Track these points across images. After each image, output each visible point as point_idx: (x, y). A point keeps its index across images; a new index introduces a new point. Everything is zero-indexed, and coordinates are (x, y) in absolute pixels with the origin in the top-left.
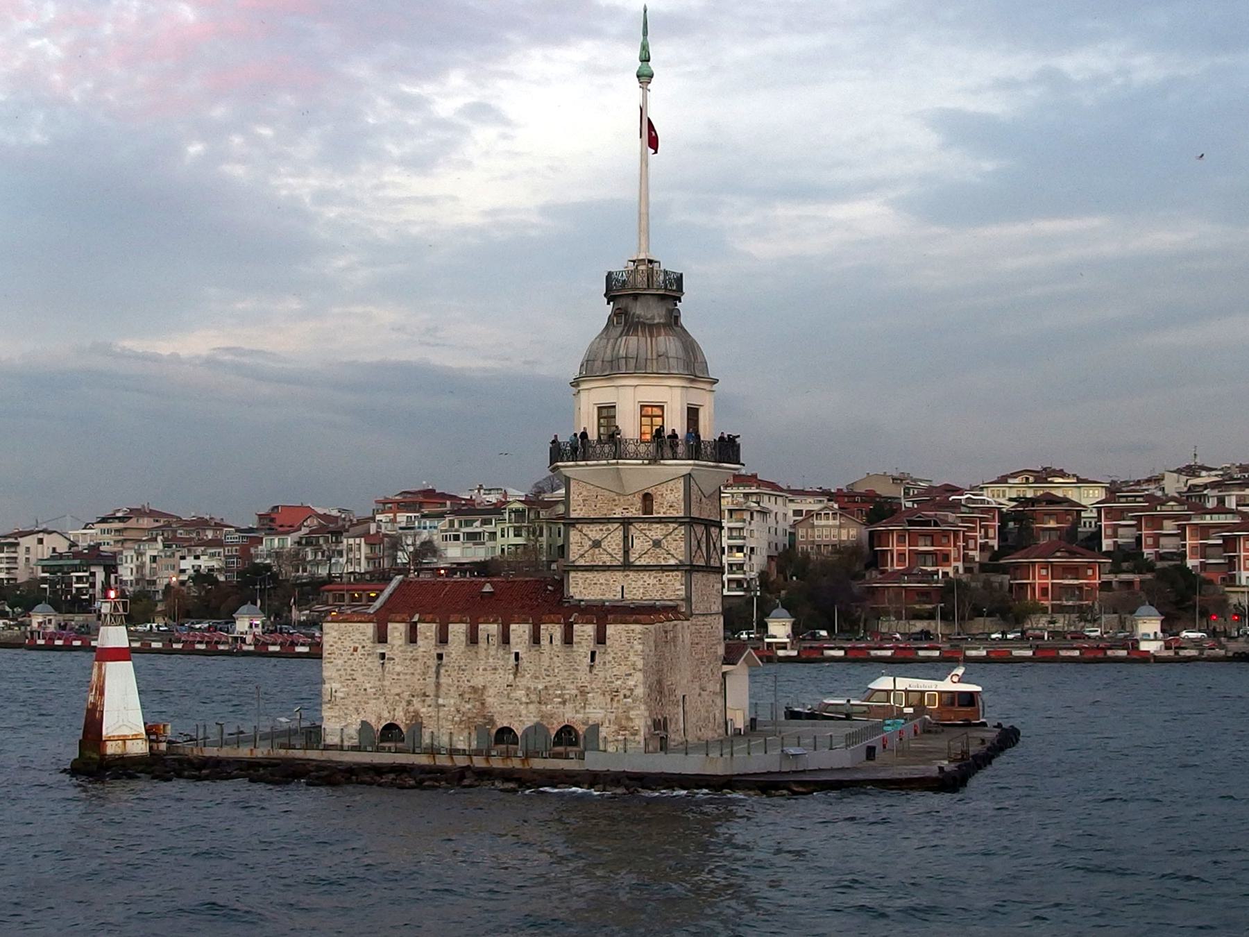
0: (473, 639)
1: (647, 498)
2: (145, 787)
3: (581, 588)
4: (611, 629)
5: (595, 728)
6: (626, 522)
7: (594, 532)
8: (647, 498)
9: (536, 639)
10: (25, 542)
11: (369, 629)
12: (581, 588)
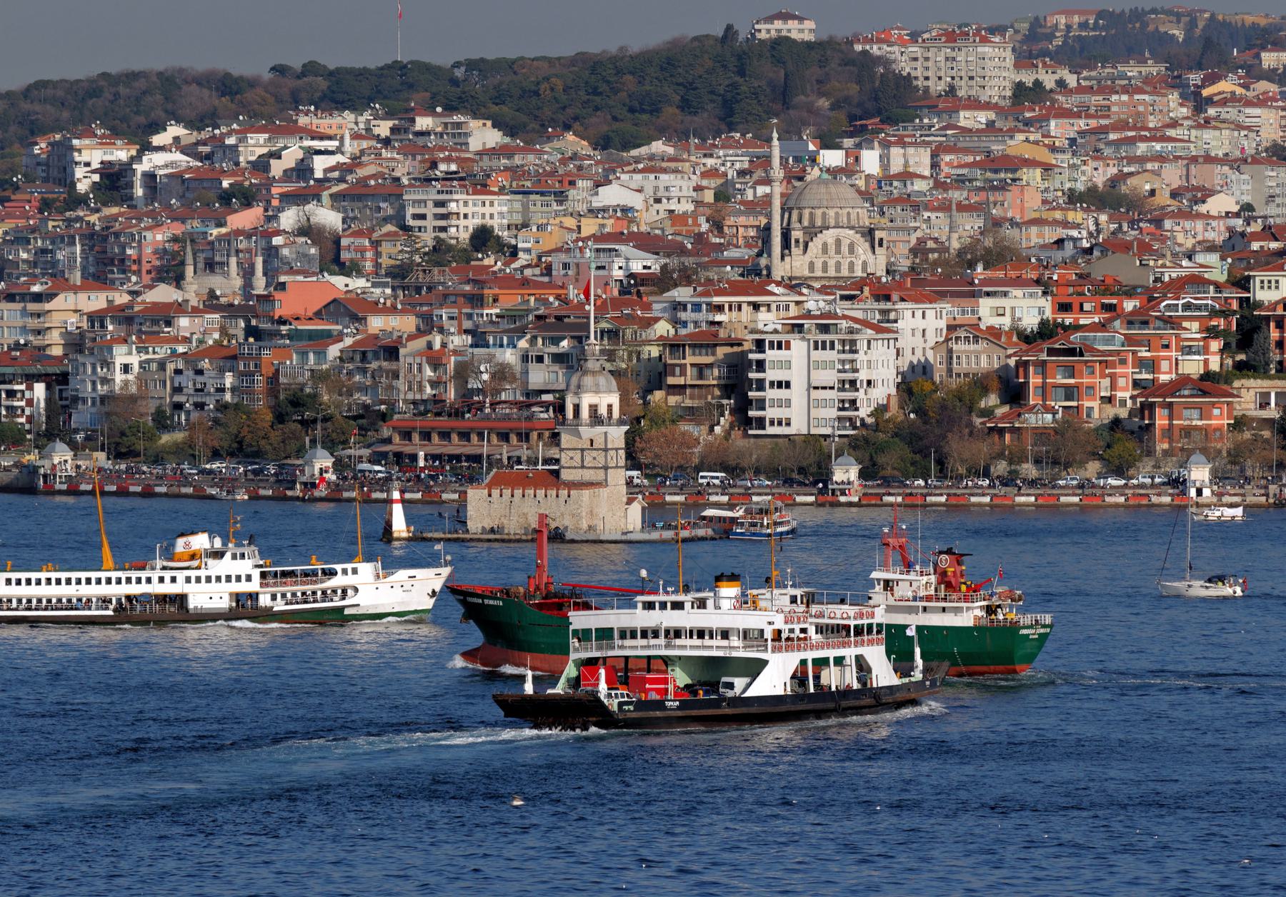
1: (592, 441)
6: (582, 450)
7: (571, 453)
8: (592, 441)
12: (566, 475)
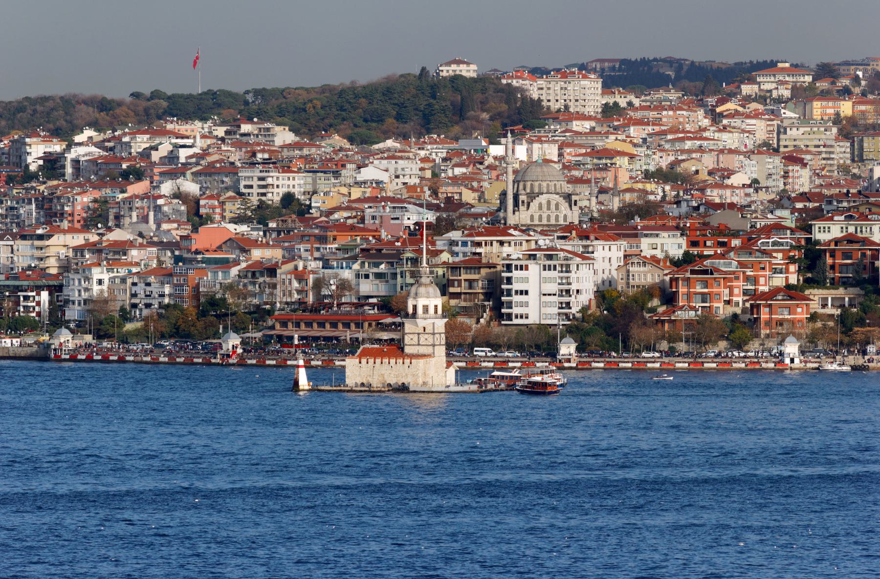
4: (413, 361)
6: (419, 334)
7: (411, 336)
11: (358, 360)
12: (407, 350)
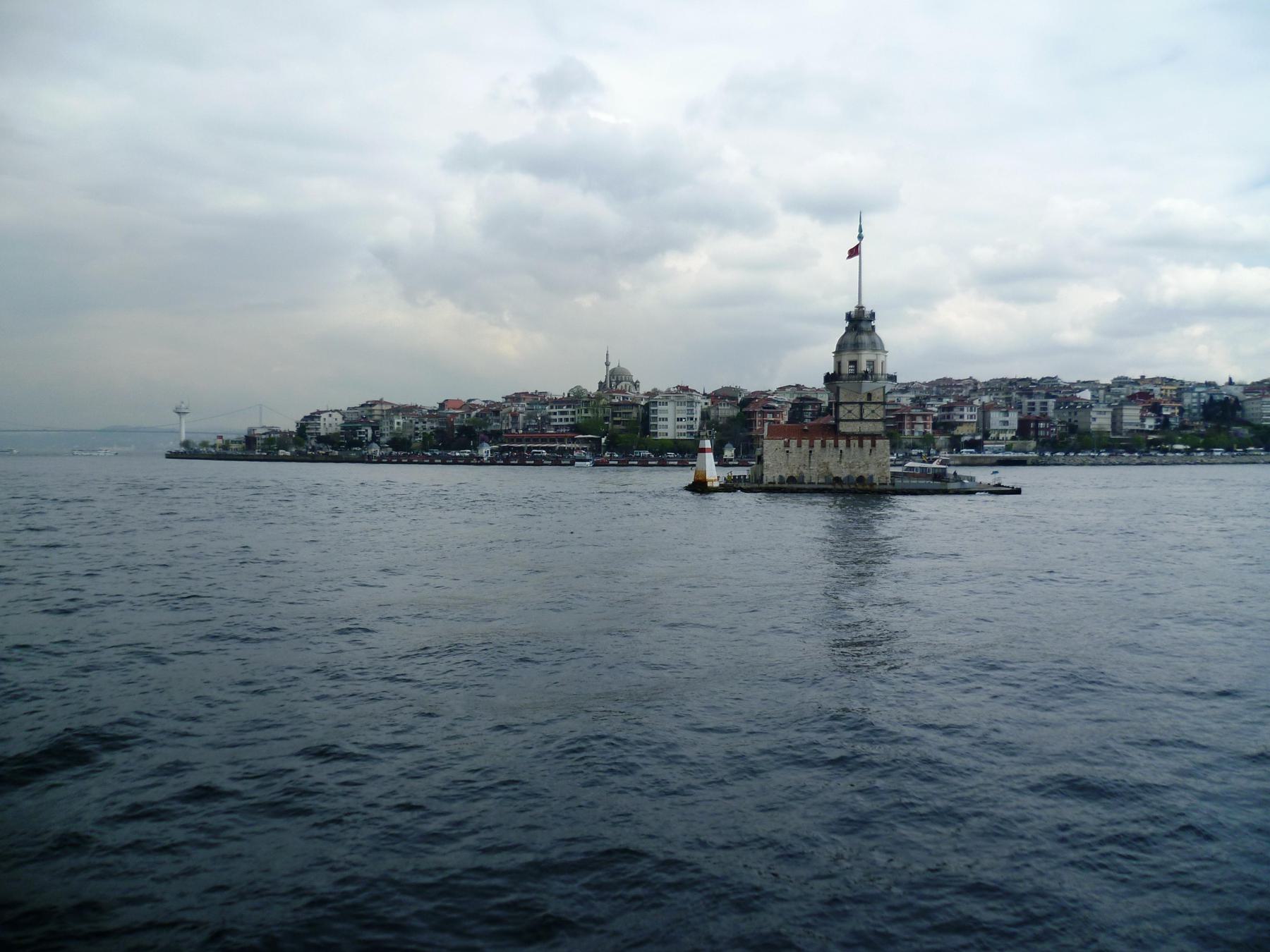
0: (823, 445)
1: (869, 395)
2: (723, 497)
3: (843, 427)
5: (871, 477)
6: (861, 404)
7: (849, 407)
8: (869, 395)
9: (848, 445)
10: (323, 416)
12: (843, 427)
